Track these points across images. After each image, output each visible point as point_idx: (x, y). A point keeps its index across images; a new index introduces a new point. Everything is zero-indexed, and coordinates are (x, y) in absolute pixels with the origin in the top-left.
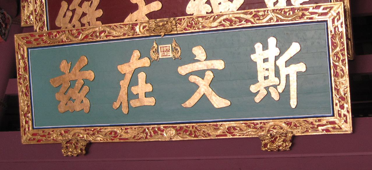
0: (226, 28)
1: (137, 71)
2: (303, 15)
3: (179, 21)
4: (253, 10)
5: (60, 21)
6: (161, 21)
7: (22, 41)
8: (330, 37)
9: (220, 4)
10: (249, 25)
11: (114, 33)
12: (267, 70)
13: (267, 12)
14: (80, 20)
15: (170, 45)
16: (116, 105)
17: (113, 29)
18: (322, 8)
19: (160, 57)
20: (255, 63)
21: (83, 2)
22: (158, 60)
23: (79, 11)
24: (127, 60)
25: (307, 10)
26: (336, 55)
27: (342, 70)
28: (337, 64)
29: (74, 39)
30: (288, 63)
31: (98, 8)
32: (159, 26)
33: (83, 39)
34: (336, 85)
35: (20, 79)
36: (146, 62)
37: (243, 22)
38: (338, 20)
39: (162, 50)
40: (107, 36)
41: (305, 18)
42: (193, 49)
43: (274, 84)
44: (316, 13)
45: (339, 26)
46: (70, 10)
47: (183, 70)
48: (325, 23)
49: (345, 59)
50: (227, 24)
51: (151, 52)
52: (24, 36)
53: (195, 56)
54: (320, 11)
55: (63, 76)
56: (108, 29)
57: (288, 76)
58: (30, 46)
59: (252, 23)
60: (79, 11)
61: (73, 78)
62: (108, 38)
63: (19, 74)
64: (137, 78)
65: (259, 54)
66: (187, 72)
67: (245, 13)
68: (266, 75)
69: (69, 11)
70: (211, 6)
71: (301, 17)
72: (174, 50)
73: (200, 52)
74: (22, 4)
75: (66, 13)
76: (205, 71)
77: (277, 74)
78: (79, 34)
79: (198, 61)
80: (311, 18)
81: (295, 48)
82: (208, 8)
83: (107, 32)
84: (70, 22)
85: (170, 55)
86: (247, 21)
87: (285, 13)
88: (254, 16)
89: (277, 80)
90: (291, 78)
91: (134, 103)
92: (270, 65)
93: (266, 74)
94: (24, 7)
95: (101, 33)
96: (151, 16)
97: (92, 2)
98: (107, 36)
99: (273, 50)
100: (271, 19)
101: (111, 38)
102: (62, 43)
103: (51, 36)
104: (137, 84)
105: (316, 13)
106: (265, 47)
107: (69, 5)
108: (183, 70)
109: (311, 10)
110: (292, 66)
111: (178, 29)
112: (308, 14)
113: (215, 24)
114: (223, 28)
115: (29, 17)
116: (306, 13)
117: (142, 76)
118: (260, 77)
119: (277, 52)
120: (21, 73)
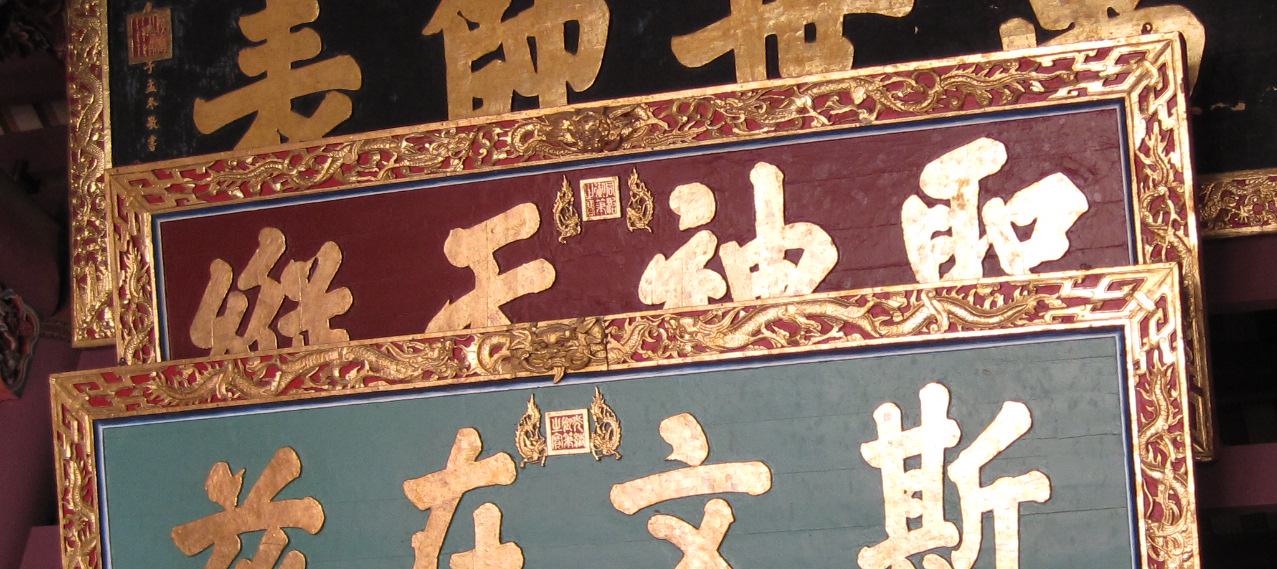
0: (775, 352)
1: (469, 500)
2: (1042, 307)
3: (613, 330)
4: (868, 291)
5: (206, 329)
6: (552, 329)
7: (75, 398)
8: (1132, 382)
9: (754, 269)
10: (856, 340)
11: (392, 370)
12: (918, 495)
13: (918, 298)
14: (273, 326)
15: (584, 412)
17: (389, 355)
18: (1105, 282)
19: (550, 451)
20: (877, 473)
21: (286, 263)
22: (544, 464)
23: (273, 294)
24: (435, 461)
25: (1053, 289)
26: (1154, 444)
27: (1175, 498)
28: (1156, 475)
29: (254, 390)
30: (989, 474)
31: (335, 284)
32: (547, 346)
33: (284, 391)
34: (1155, 549)
35: (67, 526)
36: (500, 469)
37: (834, 333)
38: (1160, 326)
39: (557, 429)
40: (366, 380)
41: (1048, 316)
42: (663, 424)
43: (941, 543)
44: (1083, 301)
45: (1165, 346)
46: (241, 291)
47: (629, 497)
48: (1117, 336)
49: (1184, 459)
50: (780, 337)
51: (520, 435)
52: (82, 381)
53: (670, 449)
54: (1100, 293)
55: (218, 517)
56: (370, 357)
57: (987, 518)
58: (104, 413)
59: (866, 335)
60: (273, 294)
61: (251, 522)
62: (372, 387)
63: (66, 511)
64: (471, 525)
65: (889, 443)
66: (644, 504)
67: (842, 302)
68: (913, 515)
69: (237, 292)
70: (725, 277)
71: (1033, 316)
72: (598, 427)
73: (687, 433)
74: (76, 270)
75: (225, 301)
76: (703, 499)
77: (952, 509)
78: (271, 372)
79: (680, 465)
80: (1068, 319)
81: (1012, 421)
82: (715, 285)
83: (367, 367)
84: (241, 330)
85: (585, 443)
86: (848, 328)
87: (979, 299)
88: (873, 312)
89: (950, 529)
90: (999, 526)
92: (928, 478)
93: (915, 509)
94: (82, 279)
95: (345, 369)
96: (518, 309)
97: (315, 263)
98: (366, 380)
99: (937, 427)
100: (930, 321)
101: (382, 386)
102: (214, 405)
103: (176, 380)
104: (469, 544)
105: (1083, 301)
106: (911, 418)
107: (236, 274)
108: (629, 497)
109: (1067, 290)
110: (1004, 483)
111: (611, 356)
112: (1058, 303)
113: (739, 338)
114: (764, 352)
115: (100, 315)
116: (1051, 300)
117: (487, 518)
118: (894, 522)
119: (951, 433)
120: (71, 507)
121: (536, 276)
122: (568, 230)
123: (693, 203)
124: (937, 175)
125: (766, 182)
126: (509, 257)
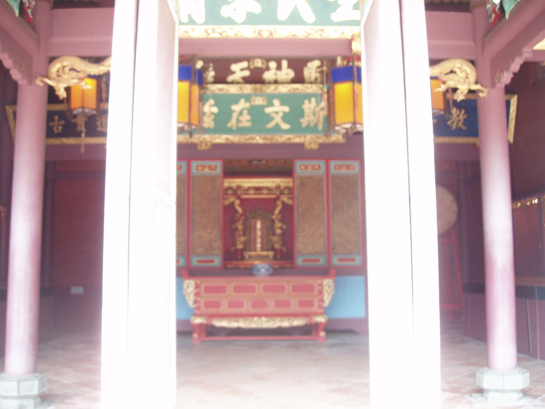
16: (229, 125)
47: (268, 110)
72: (264, 100)
91: (241, 125)
96: (247, 80)
108: (268, 110)
121: (247, 73)
122: (252, 67)
123: (273, 65)
124: (310, 65)
125: (285, 63)
126: (242, 70)
